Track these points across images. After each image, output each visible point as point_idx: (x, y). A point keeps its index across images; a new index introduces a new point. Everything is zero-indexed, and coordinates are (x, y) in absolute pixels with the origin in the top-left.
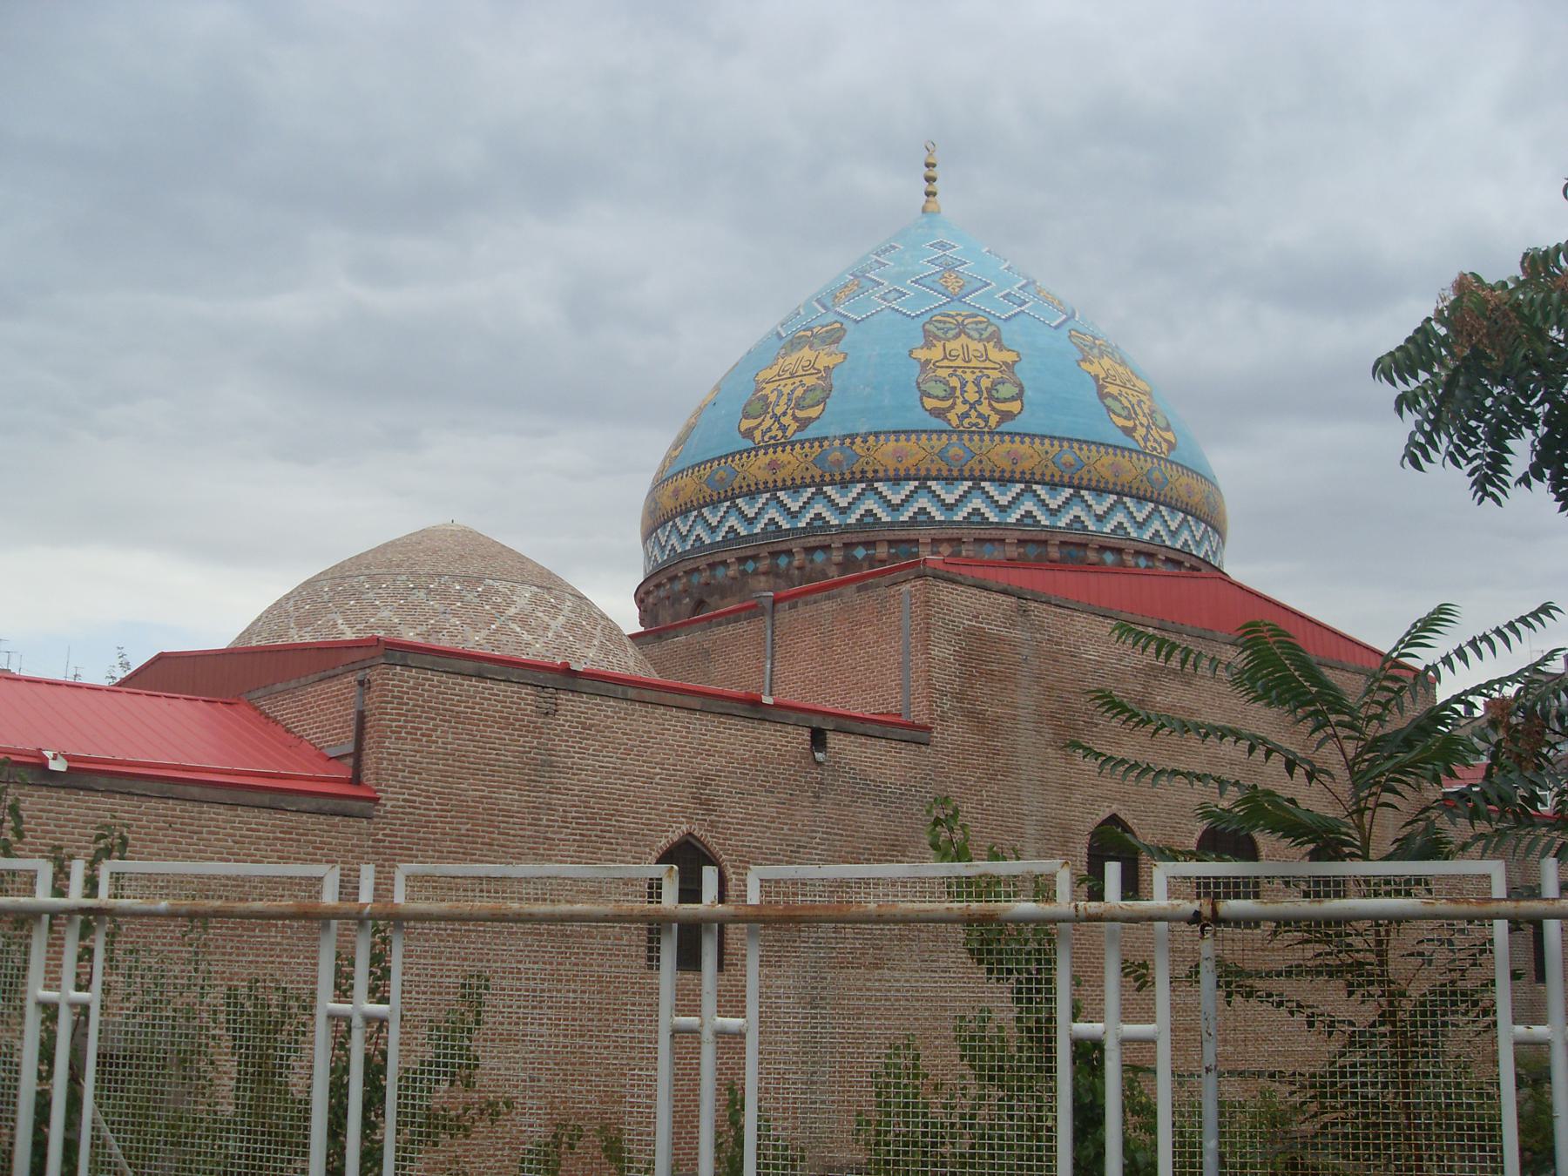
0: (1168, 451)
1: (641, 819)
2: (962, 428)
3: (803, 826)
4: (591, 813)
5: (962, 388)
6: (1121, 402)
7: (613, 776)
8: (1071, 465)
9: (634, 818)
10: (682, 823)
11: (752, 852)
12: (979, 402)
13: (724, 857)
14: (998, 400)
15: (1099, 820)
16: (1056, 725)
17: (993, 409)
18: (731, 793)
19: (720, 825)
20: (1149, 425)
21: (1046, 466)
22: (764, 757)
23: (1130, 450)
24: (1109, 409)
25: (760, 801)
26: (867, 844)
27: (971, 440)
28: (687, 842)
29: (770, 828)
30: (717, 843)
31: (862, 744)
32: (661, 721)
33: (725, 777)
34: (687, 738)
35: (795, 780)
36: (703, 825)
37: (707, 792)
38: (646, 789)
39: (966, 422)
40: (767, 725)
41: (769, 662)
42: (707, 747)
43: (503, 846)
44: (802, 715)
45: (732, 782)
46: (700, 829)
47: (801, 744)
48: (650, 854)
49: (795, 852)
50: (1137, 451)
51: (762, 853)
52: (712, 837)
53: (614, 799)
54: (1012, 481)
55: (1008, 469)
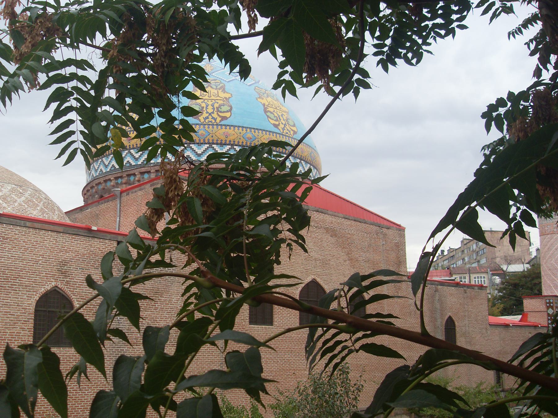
0: (293, 134)
1: (32, 279)
2: (205, 123)
4: (6, 277)
5: (206, 107)
6: (274, 114)
7: (18, 260)
8: (251, 138)
9: (28, 279)
10: (52, 282)
11: (87, 295)
12: (213, 113)
13: (73, 297)
14: (221, 112)
17: (219, 115)
18: (77, 269)
19: (71, 283)
20: (285, 124)
21: (240, 139)
22: (94, 253)
23: (276, 133)
24: (268, 116)
26: (144, 292)
27: (209, 128)
28: (55, 290)
30: (70, 291)
32: (43, 237)
33: (74, 262)
34: (56, 244)
36: (63, 283)
38: (35, 267)
39: (207, 121)
40: (96, 239)
41: (118, 218)
42: (66, 249)
44: (113, 236)
45: (78, 264)
46: (62, 285)
47: (112, 248)
48: (36, 295)
50: (279, 134)
52: (67, 288)
53: (18, 271)
54: (225, 144)
55: (224, 139)
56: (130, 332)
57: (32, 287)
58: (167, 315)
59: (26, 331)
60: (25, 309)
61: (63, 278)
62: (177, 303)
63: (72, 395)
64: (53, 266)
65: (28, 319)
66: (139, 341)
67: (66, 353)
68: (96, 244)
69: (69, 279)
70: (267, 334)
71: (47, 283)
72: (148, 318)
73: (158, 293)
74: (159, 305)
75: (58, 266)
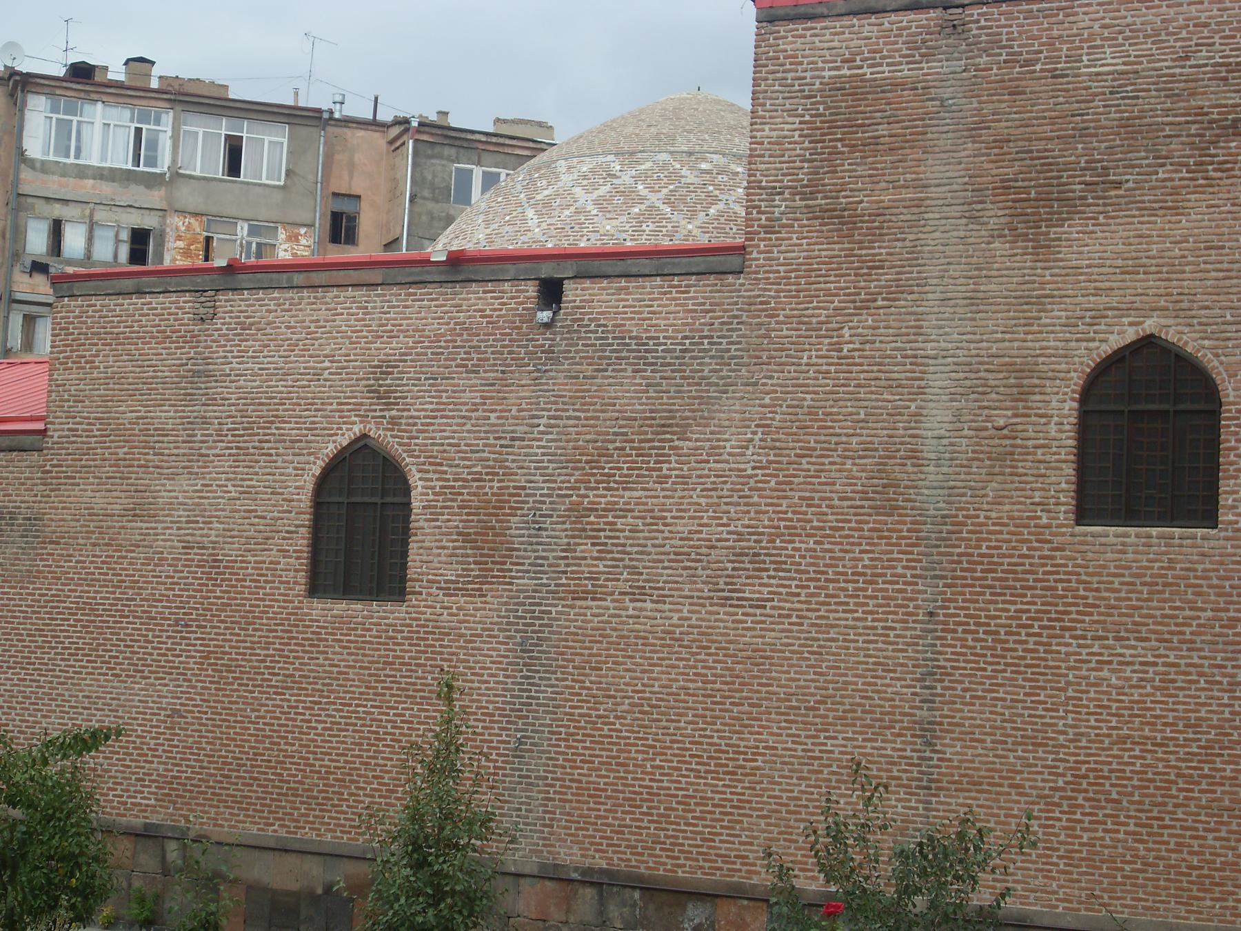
3: (520, 411)
4: (248, 423)
9: (296, 423)
10: (354, 423)
11: (444, 451)
13: (408, 460)
15: (1106, 349)
16: (1014, 201)
18: (419, 379)
19: (403, 421)
22: (466, 329)
25: (458, 385)
29: (470, 418)
30: (400, 444)
31: (621, 289)
33: (412, 361)
35: (510, 353)
37: (388, 382)
38: (313, 388)
42: (389, 327)
43: (158, 467)
44: (522, 266)
45: (421, 366)
48: (315, 463)
49: (507, 446)
51: (459, 452)
52: (392, 436)
56: (573, 558)
57: (307, 442)
58: (703, 501)
59: (291, 557)
60: (290, 501)
61: (381, 410)
62: (743, 455)
63: (401, 734)
64: (357, 380)
65: (297, 526)
66: (601, 586)
67: (385, 618)
68: (473, 301)
69: (398, 410)
70: (1170, 560)
71: (341, 429)
72: (632, 511)
73: (669, 426)
74: (674, 465)
75: (369, 379)
